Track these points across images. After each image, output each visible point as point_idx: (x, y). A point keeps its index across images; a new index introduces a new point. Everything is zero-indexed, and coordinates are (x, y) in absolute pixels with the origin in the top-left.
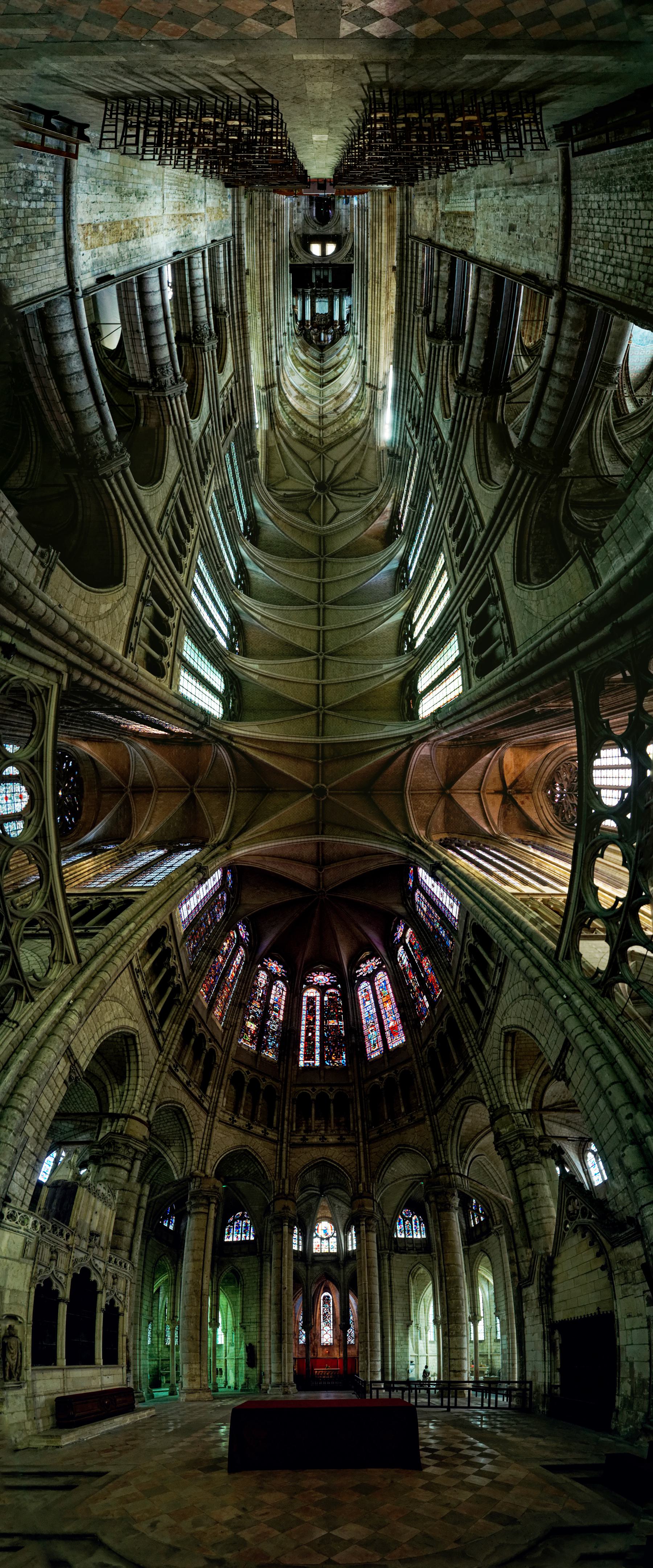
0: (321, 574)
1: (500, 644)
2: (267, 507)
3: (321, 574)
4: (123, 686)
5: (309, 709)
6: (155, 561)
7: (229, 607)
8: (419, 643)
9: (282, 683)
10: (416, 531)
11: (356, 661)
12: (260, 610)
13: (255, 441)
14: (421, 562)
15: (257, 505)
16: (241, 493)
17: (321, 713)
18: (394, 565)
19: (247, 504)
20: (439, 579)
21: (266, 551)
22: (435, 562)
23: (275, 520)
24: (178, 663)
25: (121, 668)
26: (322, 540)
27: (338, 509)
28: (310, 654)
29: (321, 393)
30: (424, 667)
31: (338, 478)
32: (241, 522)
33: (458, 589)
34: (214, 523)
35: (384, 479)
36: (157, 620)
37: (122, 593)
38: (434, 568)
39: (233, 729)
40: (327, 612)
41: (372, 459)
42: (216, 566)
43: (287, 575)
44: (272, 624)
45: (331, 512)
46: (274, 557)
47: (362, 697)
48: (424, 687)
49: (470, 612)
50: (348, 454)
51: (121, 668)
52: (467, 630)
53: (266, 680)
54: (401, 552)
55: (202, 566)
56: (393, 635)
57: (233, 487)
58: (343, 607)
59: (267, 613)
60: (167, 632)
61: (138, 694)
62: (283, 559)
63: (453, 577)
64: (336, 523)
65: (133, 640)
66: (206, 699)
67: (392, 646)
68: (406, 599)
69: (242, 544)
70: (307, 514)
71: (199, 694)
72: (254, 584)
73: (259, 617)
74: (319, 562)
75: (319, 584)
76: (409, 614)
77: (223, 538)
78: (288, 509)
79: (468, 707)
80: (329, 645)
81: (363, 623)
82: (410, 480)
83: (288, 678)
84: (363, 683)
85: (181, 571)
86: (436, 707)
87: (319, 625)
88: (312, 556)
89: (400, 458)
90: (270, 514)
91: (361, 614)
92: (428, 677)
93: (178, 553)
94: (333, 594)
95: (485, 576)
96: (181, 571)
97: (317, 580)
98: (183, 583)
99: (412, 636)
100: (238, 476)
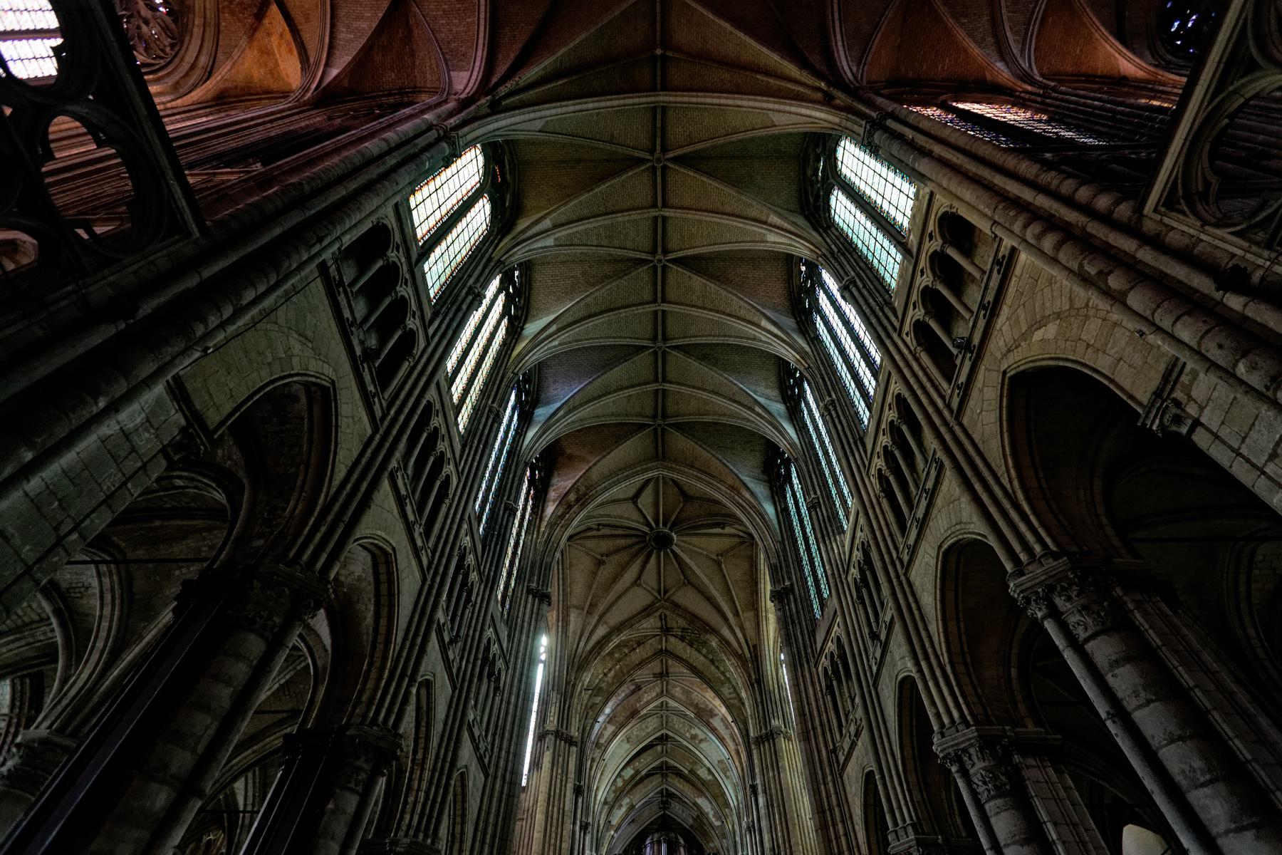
0: (661, 397)
1: (352, 284)
2: (753, 507)
3: (661, 397)
4: (1027, 194)
5: (680, 160)
6: (946, 413)
7: (815, 340)
8: (495, 284)
9: (728, 209)
10: (505, 469)
11: (602, 251)
12: (763, 336)
13: (778, 619)
14: (498, 418)
15: (770, 509)
16: (797, 529)
17: (658, 154)
18: (541, 413)
19: (786, 510)
20: (466, 391)
21: (753, 434)
22: (473, 418)
23: (737, 484)
24: (913, 240)
25: (1025, 227)
26: (660, 453)
27: (635, 503)
28: (678, 261)
29: (665, 723)
30: (483, 242)
31: (635, 556)
32: (795, 481)
33: (434, 376)
34: (841, 480)
35: (558, 555)
36: (945, 315)
37: (1011, 359)
38: (476, 409)
39: (821, 117)
40: (649, 334)
41: (578, 589)
42: (838, 408)
43: (716, 393)
44: (742, 313)
45: (646, 499)
46: (739, 423)
47: (588, 187)
48: (479, 206)
49: (410, 337)
50: (619, 597)
51: (1025, 227)
52: (414, 307)
53: (754, 213)
54: (531, 434)
55: (861, 407)
56: (539, 296)
57: (812, 540)
58: (623, 342)
59: (751, 330)
60: (929, 295)
61: (999, 180)
62: (724, 420)
63: (444, 393)
64: (638, 480)
65: (996, 278)
66: (867, 174)
67: (541, 278)
68: (521, 356)
69: (792, 445)
70: (686, 496)
71: (879, 184)
72: (773, 379)
73: (764, 323)
74: (664, 416)
75: (664, 381)
76: (514, 333)
77: (826, 453)
78: (718, 502)
79: (395, 169)
80: (646, 278)
81: (590, 316)
82: (514, 553)
83: (716, 219)
84: (585, 212)
85: (899, 398)
86: (453, 168)
87: (664, 312)
88: (677, 426)
89: (528, 592)
90: (747, 496)
91: (595, 332)
92: (475, 224)
93: (904, 428)
94: (641, 364)
95: (387, 395)
96: (899, 398)
97: (667, 386)
98: (895, 377)
99: (508, 295)
100: (805, 558)
